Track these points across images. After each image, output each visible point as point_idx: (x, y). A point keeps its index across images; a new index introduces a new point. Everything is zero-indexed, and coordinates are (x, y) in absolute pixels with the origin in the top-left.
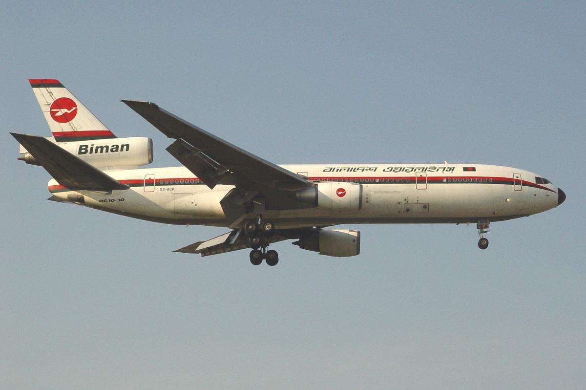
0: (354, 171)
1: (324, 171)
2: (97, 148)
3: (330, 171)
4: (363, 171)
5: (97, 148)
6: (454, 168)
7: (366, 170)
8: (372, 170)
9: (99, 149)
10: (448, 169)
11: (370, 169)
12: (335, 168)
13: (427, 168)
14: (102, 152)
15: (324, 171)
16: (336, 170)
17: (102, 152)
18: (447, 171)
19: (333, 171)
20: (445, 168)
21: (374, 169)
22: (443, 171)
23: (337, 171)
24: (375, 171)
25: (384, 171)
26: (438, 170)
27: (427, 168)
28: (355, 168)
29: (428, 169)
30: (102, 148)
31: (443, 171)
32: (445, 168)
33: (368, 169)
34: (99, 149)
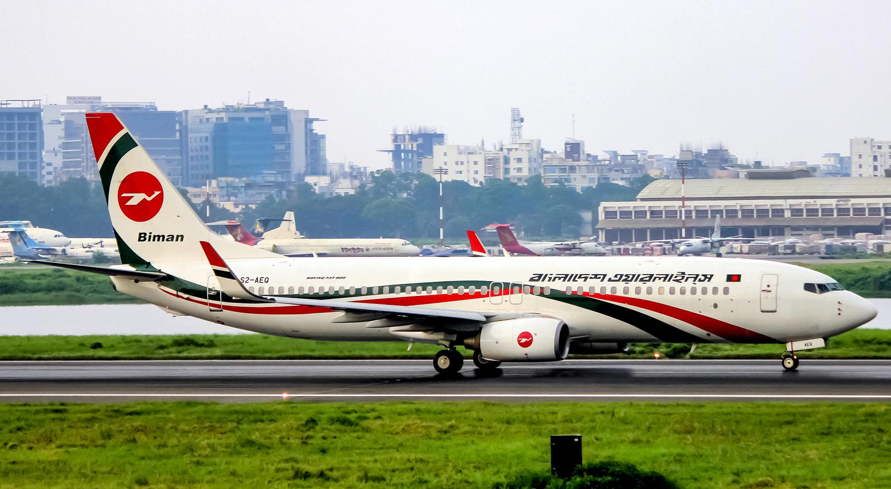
2: (155, 237)
5: (155, 237)
9: (157, 238)
14: (158, 240)
17: (158, 240)
25: (610, 280)
30: (159, 236)
34: (157, 238)
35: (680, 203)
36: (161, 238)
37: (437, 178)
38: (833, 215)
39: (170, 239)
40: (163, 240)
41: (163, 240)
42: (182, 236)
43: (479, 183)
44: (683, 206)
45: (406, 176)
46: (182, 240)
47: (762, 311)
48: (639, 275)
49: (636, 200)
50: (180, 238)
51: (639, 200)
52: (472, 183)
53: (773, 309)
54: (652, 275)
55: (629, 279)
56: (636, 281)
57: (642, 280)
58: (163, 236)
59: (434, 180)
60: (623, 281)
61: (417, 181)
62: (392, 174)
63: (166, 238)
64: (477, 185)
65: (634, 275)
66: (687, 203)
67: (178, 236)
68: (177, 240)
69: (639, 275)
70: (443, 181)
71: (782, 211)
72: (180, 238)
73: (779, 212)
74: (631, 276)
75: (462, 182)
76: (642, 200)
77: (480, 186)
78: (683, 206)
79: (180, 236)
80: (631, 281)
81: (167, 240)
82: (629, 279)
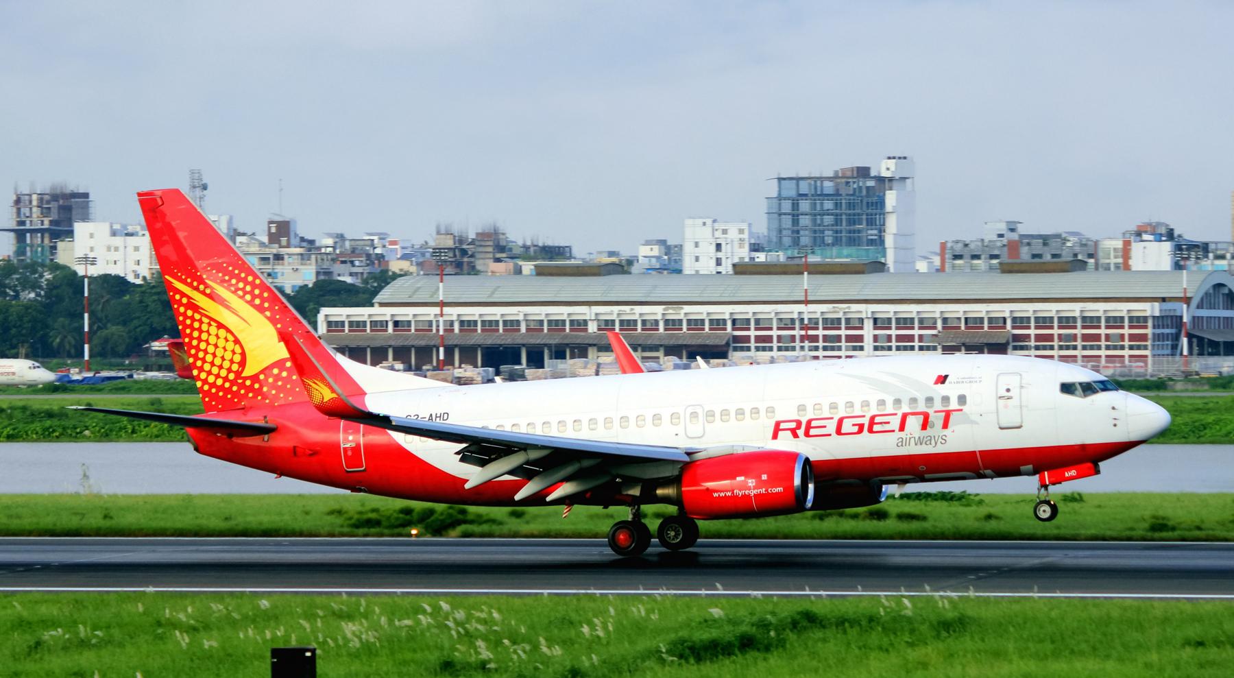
35: (437, 310)
37: (81, 271)
38: (657, 330)
43: (141, 278)
44: (442, 315)
45: (33, 267)
49: (372, 305)
51: (376, 305)
52: (131, 279)
59: (75, 273)
61: (50, 274)
62: (13, 264)
64: (139, 282)
66: (446, 310)
70: (89, 275)
71: (585, 322)
73: (580, 325)
75: (117, 278)
76: (382, 305)
77: (142, 283)
78: (442, 315)
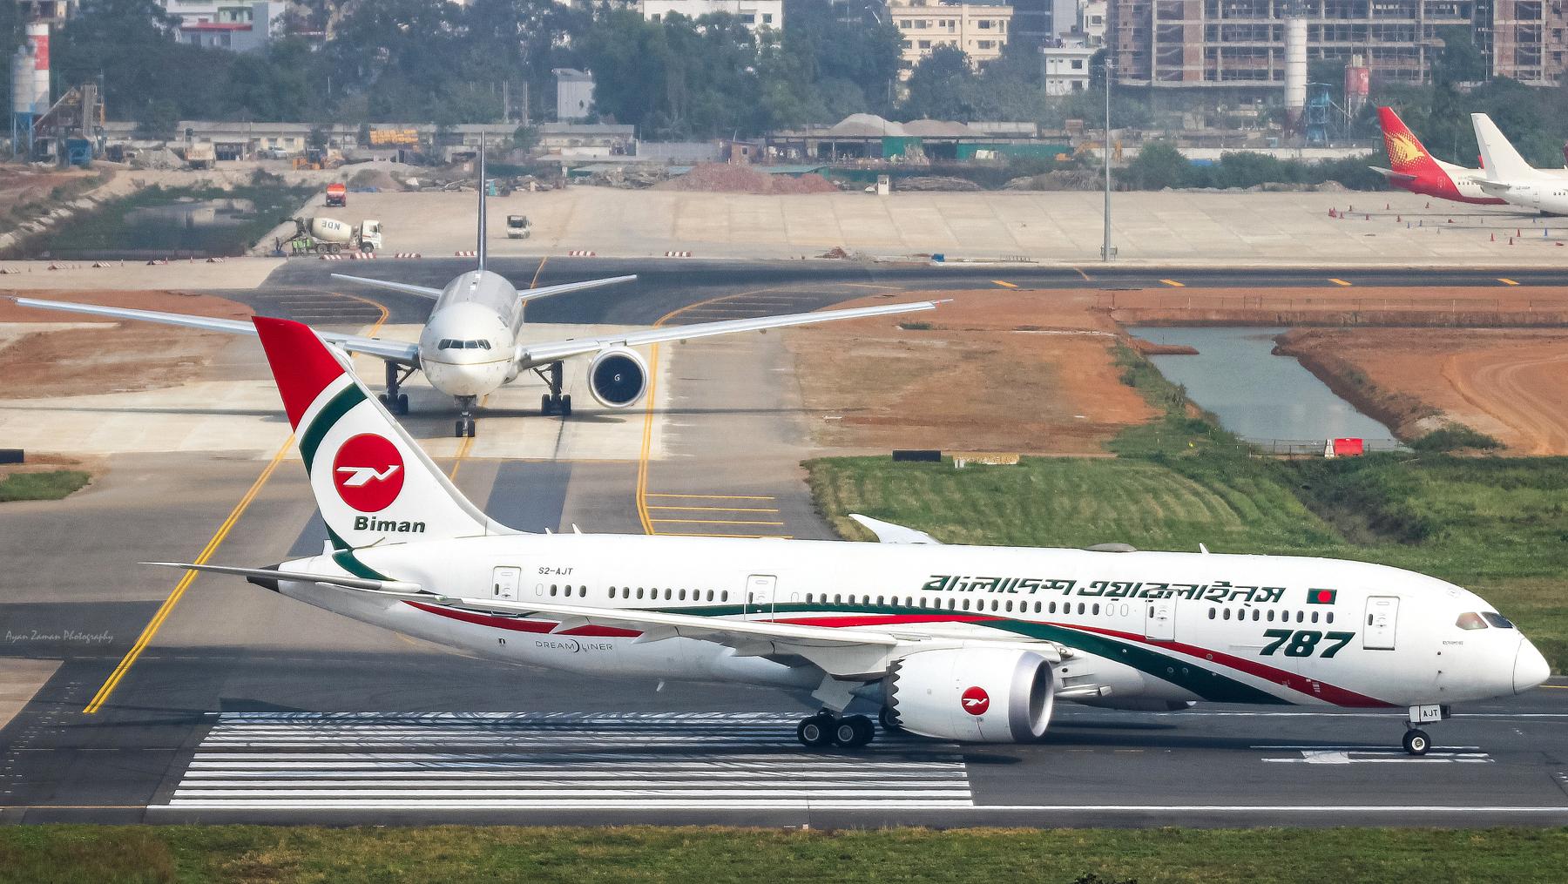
0: (1011, 591)
1: (928, 587)
2: (381, 524)
3: (941, 589)
4: (1033, 592)
5: (381, 524)
6: (1282, 591)
7: (1045, 587)
8: (1061, 587)
10: (1264, 594)
11: (1054, 586)
12: (957, 579)
13: (1204, 588)
14: (386, 529)
15: (928, 587)
16: (958, 586)
17: (386, 529)
18: (1259, 599)
19: (951, 588)
20: (1254, 589)
21: (1066, 585)
22: (1248, 599)
23: (962, 590)
24: (1067, 593)
26: (1232, 599)
27: (1204, 588)
28: (1016, 581)
29: (1206, 593)
30: (387, 524)
31: (1248, 599)
32: (1254, 589)
33: (1049, 584)
36: (390, 525)
39: (404, 529)
40: (394, 529)
41: (394, 529)
42: (423, 525)
46: (422, 531)
47: (1365, 648)
48: (1139, 585)
50: (419, 527)
53: (1391, 647)
54: (1164, 586)
55: (1117, 592)
56: (1133, 595)
57: (1144, 595)
58: (394, 524)
60: (1109, 595)
63: (398, 526)
65: (1129, 585)
67: (416, 525)
68: (415, 530)
69: (1139, 585)
72: (419, 527)
74: (1124, 587)
79: (419, 524)
80: (1124, 595)
81: (401, 530)
82: (1120, 592)
